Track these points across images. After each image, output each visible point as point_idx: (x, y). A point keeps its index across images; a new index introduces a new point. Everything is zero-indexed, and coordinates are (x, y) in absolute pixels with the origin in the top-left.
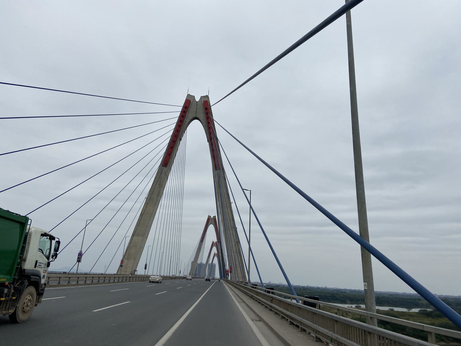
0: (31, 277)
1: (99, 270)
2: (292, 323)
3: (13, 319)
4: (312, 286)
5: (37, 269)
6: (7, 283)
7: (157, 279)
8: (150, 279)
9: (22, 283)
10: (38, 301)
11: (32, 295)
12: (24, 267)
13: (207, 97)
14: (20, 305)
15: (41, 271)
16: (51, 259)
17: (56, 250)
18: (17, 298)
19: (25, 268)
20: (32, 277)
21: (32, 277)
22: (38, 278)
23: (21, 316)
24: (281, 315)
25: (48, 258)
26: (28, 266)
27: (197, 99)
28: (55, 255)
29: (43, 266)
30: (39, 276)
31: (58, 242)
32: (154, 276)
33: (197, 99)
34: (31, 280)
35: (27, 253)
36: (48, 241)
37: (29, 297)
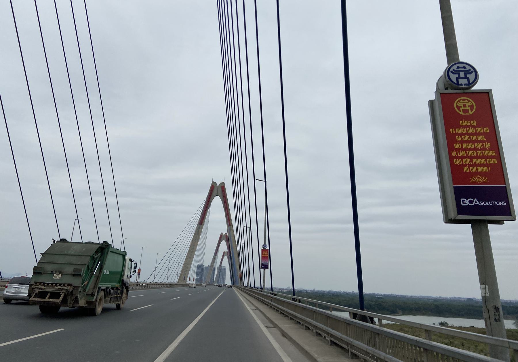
0: (126, 284)
1: (161, 279)
2: (281, 313)
5: (127, 279)
6: (119, 287)
9: (123, 288)
11: (125, 294)
12: (124, 278)
13: (223, 183)
14: (122, 300)
15: (128, 280)
16: (132, 273)
17: (135, 268)
20: (127, 284)
21: (127, 284)
22: (127, 284)
23: (122, 306)
24: (280, 311)
26: (125, 278)
27: (218, 184)
29: (129, 277)
30: (128, 283)
31: (136, 263)
32: (192, 283)
33: (218, 184)
34: (126, 286)
35: (125, 271)
36: (130, 262)
37: (125, 295)
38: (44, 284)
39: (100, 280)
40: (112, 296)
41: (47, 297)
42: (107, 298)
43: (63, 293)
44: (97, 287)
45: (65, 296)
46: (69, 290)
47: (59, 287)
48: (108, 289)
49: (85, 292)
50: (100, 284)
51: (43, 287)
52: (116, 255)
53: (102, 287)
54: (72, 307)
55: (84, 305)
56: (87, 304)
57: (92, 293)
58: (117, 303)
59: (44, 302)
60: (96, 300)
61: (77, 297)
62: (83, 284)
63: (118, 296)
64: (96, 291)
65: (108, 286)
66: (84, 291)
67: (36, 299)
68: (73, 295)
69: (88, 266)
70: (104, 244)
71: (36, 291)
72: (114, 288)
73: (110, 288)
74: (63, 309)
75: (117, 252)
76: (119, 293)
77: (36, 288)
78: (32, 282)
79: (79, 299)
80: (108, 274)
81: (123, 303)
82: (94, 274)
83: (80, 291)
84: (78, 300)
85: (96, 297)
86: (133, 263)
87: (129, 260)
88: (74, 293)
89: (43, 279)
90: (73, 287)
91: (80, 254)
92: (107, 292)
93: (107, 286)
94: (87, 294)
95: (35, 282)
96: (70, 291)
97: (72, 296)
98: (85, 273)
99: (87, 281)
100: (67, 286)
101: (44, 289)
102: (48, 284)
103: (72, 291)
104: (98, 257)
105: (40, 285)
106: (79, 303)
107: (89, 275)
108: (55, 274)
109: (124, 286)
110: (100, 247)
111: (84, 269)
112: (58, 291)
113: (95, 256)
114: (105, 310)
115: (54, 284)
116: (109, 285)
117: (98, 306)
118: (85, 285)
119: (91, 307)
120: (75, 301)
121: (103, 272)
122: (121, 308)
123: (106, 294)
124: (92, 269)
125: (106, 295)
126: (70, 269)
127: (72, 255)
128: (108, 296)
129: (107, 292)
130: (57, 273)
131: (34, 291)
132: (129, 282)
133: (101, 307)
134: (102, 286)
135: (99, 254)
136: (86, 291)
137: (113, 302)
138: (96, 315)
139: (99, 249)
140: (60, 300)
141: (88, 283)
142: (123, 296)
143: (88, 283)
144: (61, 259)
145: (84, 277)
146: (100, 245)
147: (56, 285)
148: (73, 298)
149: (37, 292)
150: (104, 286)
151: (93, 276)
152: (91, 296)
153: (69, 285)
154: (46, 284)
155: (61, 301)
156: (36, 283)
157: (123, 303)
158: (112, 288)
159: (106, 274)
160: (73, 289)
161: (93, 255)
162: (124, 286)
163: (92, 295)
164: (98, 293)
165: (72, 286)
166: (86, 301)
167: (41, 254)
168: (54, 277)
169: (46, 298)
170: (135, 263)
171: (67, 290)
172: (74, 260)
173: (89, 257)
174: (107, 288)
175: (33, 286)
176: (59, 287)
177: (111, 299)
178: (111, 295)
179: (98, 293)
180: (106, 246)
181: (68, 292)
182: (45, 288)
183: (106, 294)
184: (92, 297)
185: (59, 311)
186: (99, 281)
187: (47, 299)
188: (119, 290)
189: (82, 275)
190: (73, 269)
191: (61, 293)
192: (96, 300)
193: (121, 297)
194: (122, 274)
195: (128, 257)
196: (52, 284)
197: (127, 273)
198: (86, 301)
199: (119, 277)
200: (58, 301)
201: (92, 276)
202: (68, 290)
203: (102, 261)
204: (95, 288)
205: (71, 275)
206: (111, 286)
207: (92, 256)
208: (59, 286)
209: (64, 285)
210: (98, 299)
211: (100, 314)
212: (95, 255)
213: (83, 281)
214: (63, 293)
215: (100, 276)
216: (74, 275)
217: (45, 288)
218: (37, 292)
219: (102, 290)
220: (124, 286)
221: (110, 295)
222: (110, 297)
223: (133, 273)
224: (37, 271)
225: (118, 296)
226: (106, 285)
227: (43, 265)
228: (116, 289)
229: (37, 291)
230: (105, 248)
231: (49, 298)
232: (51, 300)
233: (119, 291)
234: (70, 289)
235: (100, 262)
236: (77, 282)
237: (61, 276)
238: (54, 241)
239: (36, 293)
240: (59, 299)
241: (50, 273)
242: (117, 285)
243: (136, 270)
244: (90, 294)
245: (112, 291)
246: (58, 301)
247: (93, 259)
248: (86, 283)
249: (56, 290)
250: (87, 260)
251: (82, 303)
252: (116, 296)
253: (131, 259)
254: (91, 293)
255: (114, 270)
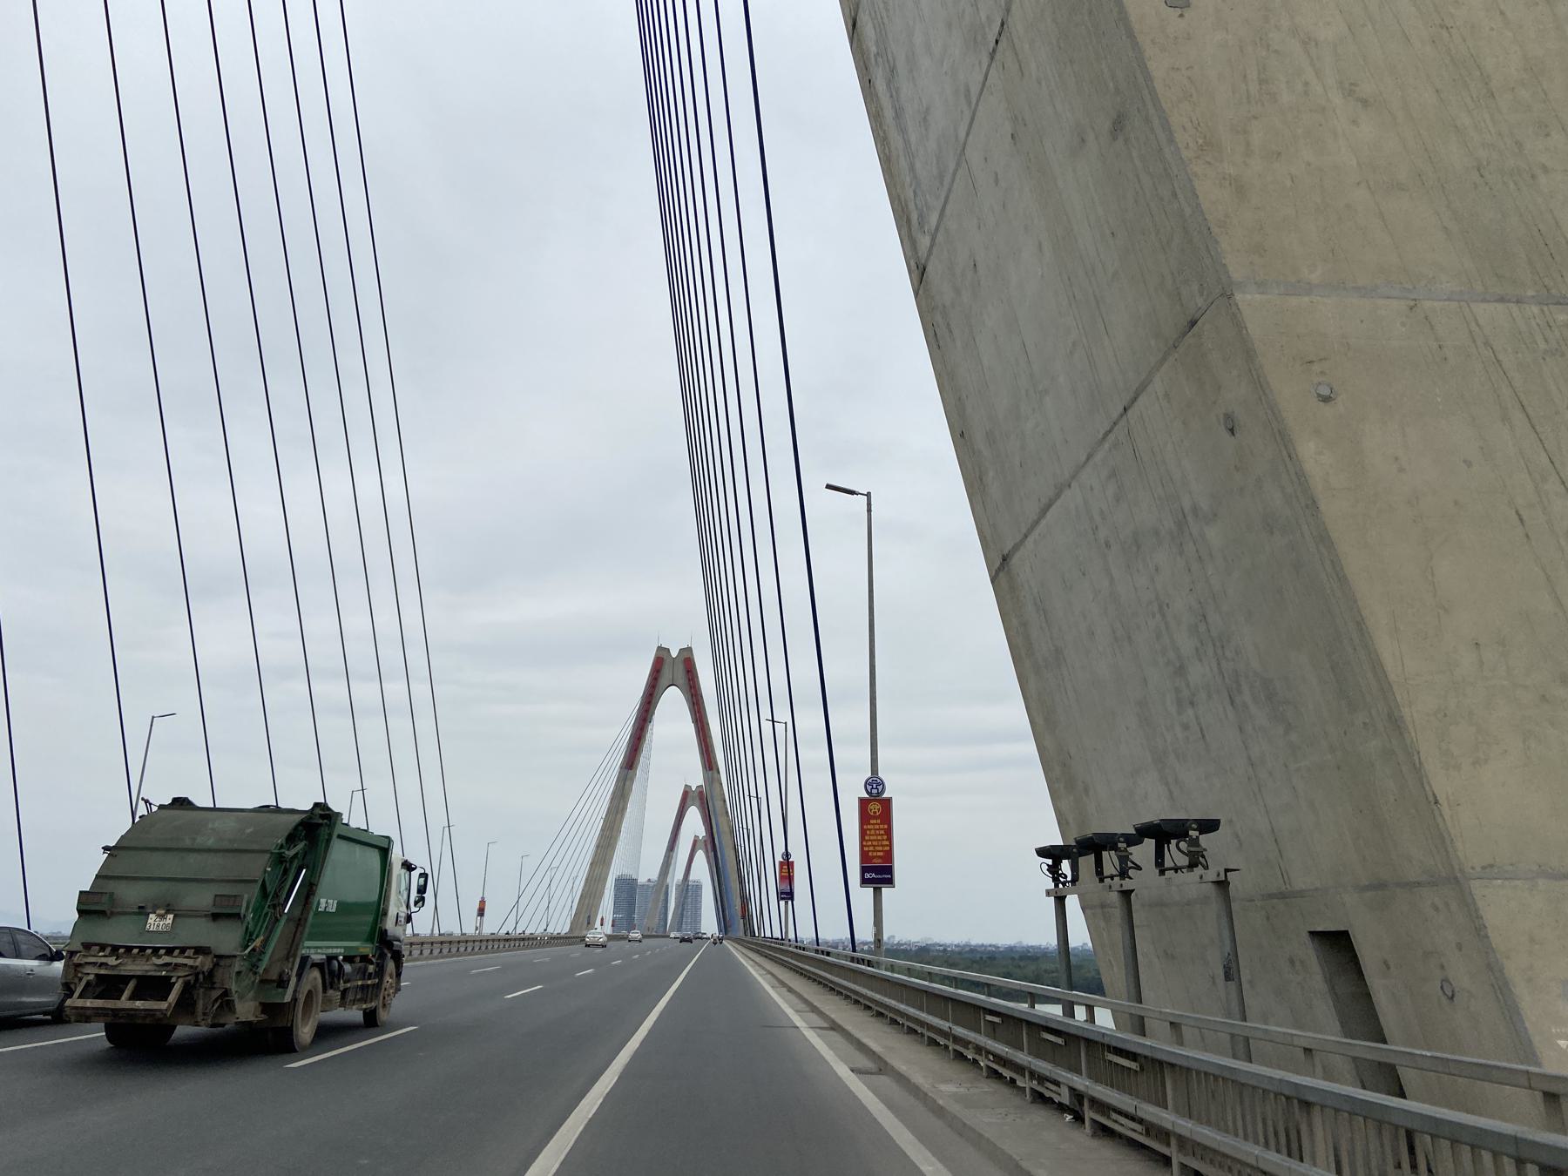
0: (393, 945)
3: (371, 1021)
4: (987, 942)
5: (398, 927)
7: (601, 940)
8: (587, 939)
9: (382, 956)
10: (398, 989)
12: (385, 925)
17: (422, 890)
18: (379, 980)
19: (387, 928)
20: (395, 943)
21: (395, 943)
23: (383, 1015)
25: (408, 906)
26: (389, 924)
28: (421, 900)
29: (403, 920)
30: (399, 941)
35: (389, 901)
37: (390, 980)
38: (115, 949)
39: (307, 930)
40: (349, 985)
41: (127, 993)
42: (330, 992)
43: (179, 977)
44: (295, 956)
45: (188, 988)
46: (198, 970)
47: (167, 959)
48: (335, 962)
49: (255, 973)
50: (308, 943)
51: (112, 961)
52: (358, 848)
53: (313, 957)
54: (213, 1026)
55: (252, 1018)
56: (263, 1012)
57: (280, 975)
58: (364, 1006)
59: (115, 1012)
60: (295, 999)
61: (226, 993)
62: (247, 946)
63: (369, 982)
64: (292, 969)
65: (335, 951)
66: (253, 968)
67: (89, 1003)
68: (215, 983)
69: (264, 885)
70: (318, 811)
71: (88, 974)
72: (355, 956)
73: (341, 957)
74: (183, 1031)
75: (361, 839)
76: (370, 974)
77: (86, 963)
78: (77, 946)
79: (235, 997)
80: (334, 910)
81: (384, 1005)
82: (286, 911)
83: (237, 969)
84: (233, 1001)
85: (295, 991)
86: (415, 874)
87: (403, 864)
88: (218, 978)
89: (115, 932)
90: (216, 956)
91: (236, 846)
92: (330, 972)
93: (330, 951)
94: (263, 981)
95: (82, 944)
96: (203, 973)
97: (214, 988)
98: (255, 911)
99: (262, 938)
100: (194, 954)
101: (116, 966)
102: (129, 949)
103: (211, 973)
104: (297, 854)
105: (101, 954)
106: (237, 1010)
107: (267, 914)
108: (151, 915)
109: (386, 951)
110: (302, 823)
111: (250, 895)
112: (164, 973)
113: (287, 852)
114: (328, 1033)
115: (149, 948)
116: (337, 947)
117: (302, 1020)
118: (254, 950)
119: (281, 1023)
120: (221, 1003)
121: (315, 904)
122: (379, 1024)
123: (327, 977)
124: (276, 895)
125: (328, 984)
126: (203, 898)
127: (209, 850)
128: (335, 987)
129: (331, 972)
130: (158, 912)
131: (80, 975)
132: (402, 938)
133: (310, 1023)
134: (312, 951)
135: (301, 846)
136: (261, 971)
137: (354, 1002)
138: (295, 1051)
139: (300, 828)
140: (170, 1004)
141: (265, 943)
142: (385, 985)
143: (265, 943)
144: (172, 865)
145: (251, 923)
146: (304, 816)
147: (156, 950)
148: (216, 994)
149: (91, 977)
150: (319, 951)
151: (285, 918)
152: (275, 984)
153: (200, 950)
154: (122, 950)
155: (173, 1005)
156: (87, 946)
157: (384, 1005)
158: (349, 959)
159: (325, 912)
160: (216, 965)
161: (282, 847)
162: (388, 949)
163: (282, 983)
164: (299, 975)
165: (211, 953)
166: (261, 1004)
167: (106, 849)
168: (148, 926)
169: (123, 998)
170: (421, 875)
171: (191, 967)
172: (215, 866)
173: (269, 855)
174: (331, 958)
175: (76, 959)
176: (167, 959)
177: (344, 993)
178: (345, 983)
179: (299, 975)
180: (322, 817)
181: (197, 975)
182: (119, 961)
183: (327, 977)
184: (280, 990)
185: (168, 1043)
186: (302, 933)
187: (124, 1002)
188: (372, 963)
189: (244, 915)
190: (212, 897)
191: (173, 980)
192: (295, 999)
193: (378, 986)
194: (380, 911)
195: (396, 856)
196: (143, 949)
197: (395, 908)
198: (260, 1003)
199: (370, 918)
200: (163, 1005)
201: (277, 920)
202: (197, 967)
203: (311, 866)
204: (291, 960)
205: (206, 916)
206: (342, 951)
207: (277, 851)
208: (166, 954)
209: (183, 950)
210: (302, 998)
211: (310, 1044)
212: (288, 850)
213: (249, 937)
214: (180, 981)
215: (306, 920)
216: (215, 917)
217: (119, 961)
218: (91, 977)
219: (314, 965)
220: (386, 951)
221: (342, 981)
222: (342, 989)
223: (415, 905)
224: (91, 906)
225: (369, 982)
226: (332, 947)
227: (111, 886)
228: (360, 962)
229: (91, 973)
230: (321, 825)
231: (133, 997)
232: (138, 1004)
233: (371, 968)
234: (203, 964)
235: (304, 871)
236: (226, 939)
237: (170, 922)
238: (150, 804)
239: (88, 984)
240: (165, 998)
241: (135, 913)
242: (367, 949)
243: (424, 898)
244: (274, 981)
245: (347, 968)
246: (163, 1005)
247: (281, 862)
248: (257, 943)
249: (155, 971)
250: (258, 867)
251: (246, 1010)
252: (360, 983)
253: (406, 861)
254: (275, 977)
255: (351, 897)
